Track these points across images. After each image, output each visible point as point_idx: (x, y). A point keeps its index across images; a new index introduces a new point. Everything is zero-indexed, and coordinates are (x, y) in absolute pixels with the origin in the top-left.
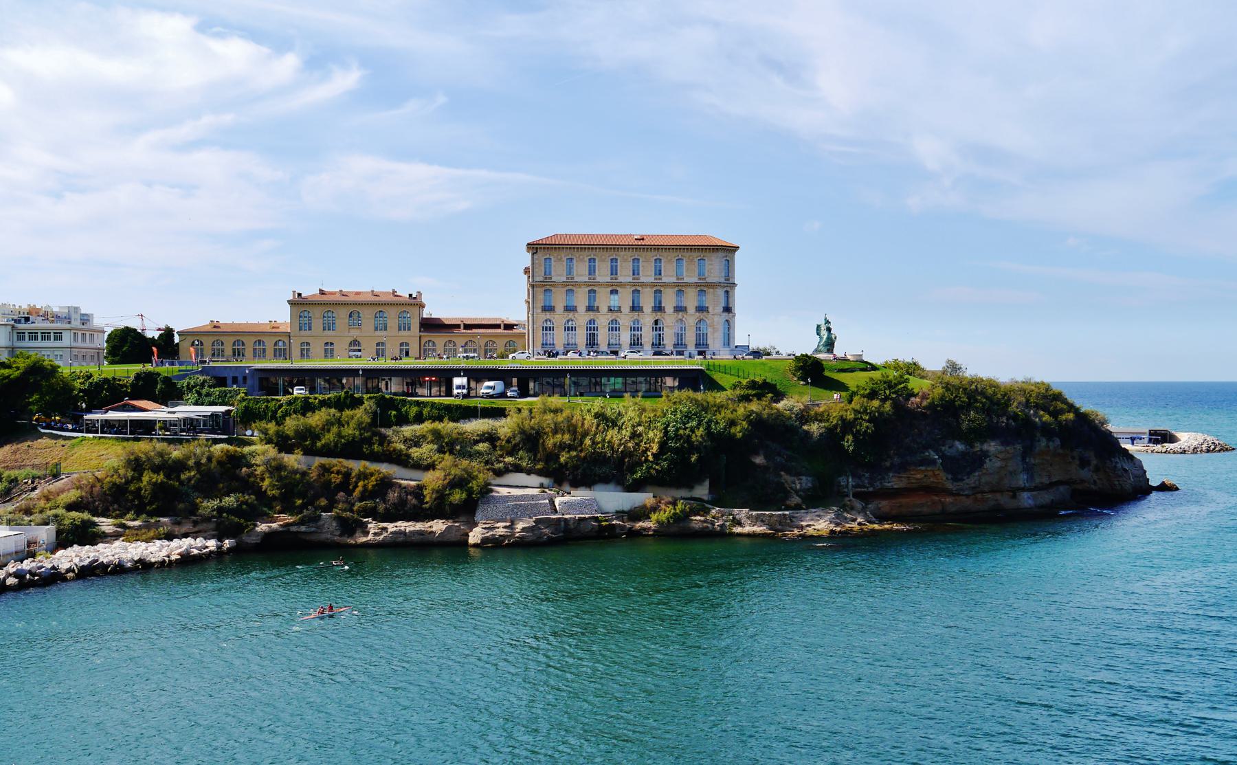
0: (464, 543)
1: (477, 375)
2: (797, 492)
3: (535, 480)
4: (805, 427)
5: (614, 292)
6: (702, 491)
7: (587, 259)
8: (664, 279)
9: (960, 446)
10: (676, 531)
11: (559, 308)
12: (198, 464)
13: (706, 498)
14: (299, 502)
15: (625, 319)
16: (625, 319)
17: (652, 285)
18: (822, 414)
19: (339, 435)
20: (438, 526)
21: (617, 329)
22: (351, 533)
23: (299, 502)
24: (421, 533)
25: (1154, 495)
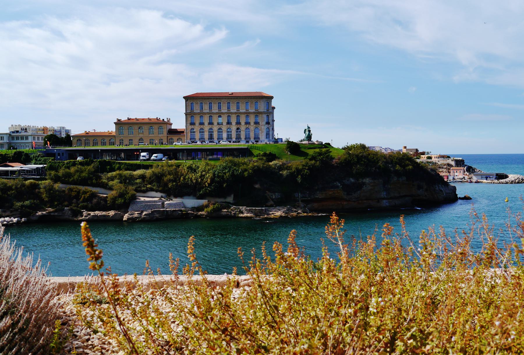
1: (151, 152)
2: (273, 200)
3: (159, 194)
4: (281, 172)
5: (220, 116)
6: (230, 199)
7: (208, 103)
8: (241, 111)
9: (352, 180)
10: (215, 216)
11: (197, 123)
12: (16, 188)
13: (232, 202)
14: (56, 203)
15: (224, 128)
16: (224, 128)
17: (235, 113)
18: (290, 167)
19: (79, 176)
20: (112, 213)
21: (203, 132)
22: (76, 216)
23: (56, 203)
24: (104, 216)
25: (460, 201)
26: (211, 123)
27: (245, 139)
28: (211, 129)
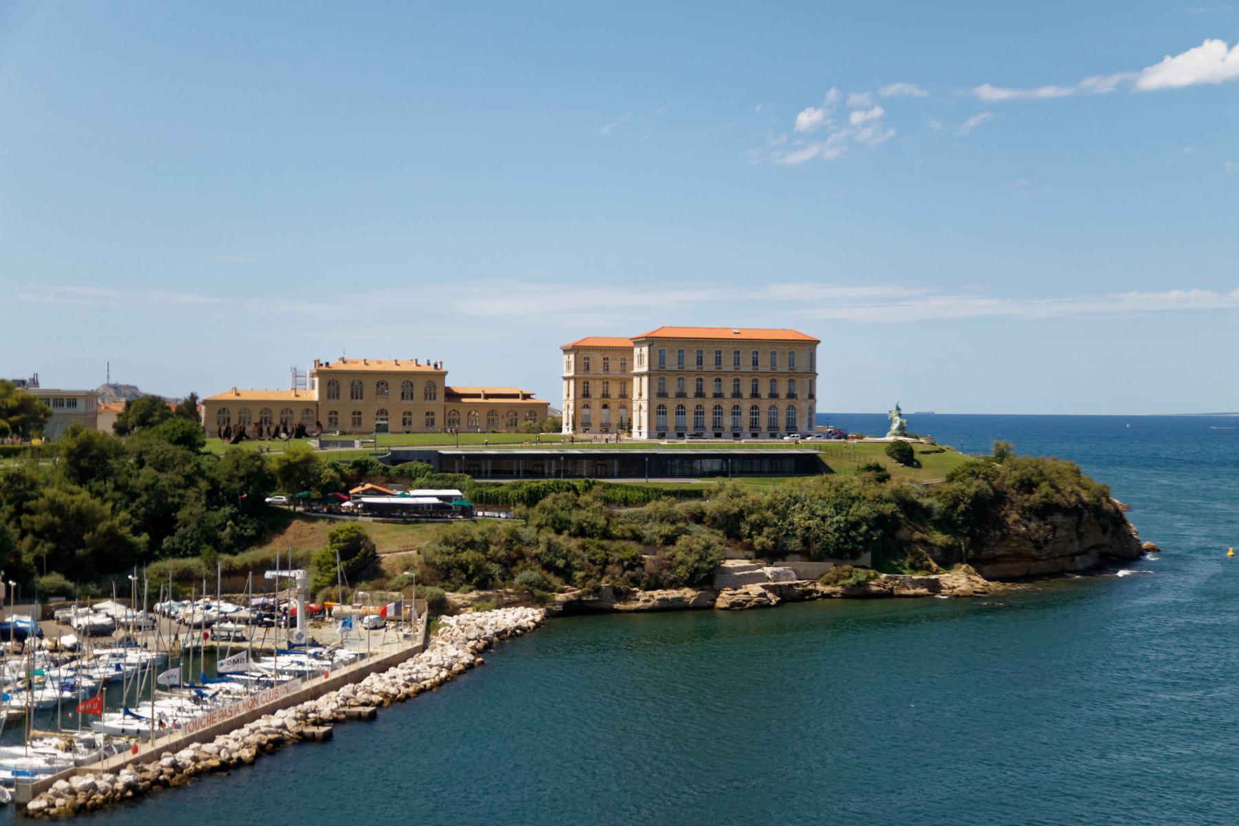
0: (712, 607)
20: (689, 594)
26: (700, 394)
27: (769, 428)
28: (718, 407)
